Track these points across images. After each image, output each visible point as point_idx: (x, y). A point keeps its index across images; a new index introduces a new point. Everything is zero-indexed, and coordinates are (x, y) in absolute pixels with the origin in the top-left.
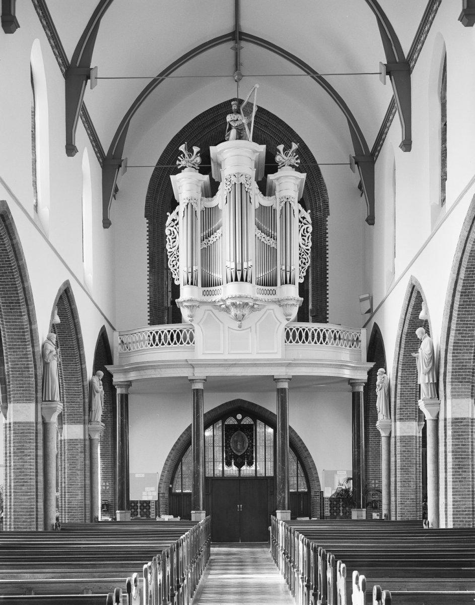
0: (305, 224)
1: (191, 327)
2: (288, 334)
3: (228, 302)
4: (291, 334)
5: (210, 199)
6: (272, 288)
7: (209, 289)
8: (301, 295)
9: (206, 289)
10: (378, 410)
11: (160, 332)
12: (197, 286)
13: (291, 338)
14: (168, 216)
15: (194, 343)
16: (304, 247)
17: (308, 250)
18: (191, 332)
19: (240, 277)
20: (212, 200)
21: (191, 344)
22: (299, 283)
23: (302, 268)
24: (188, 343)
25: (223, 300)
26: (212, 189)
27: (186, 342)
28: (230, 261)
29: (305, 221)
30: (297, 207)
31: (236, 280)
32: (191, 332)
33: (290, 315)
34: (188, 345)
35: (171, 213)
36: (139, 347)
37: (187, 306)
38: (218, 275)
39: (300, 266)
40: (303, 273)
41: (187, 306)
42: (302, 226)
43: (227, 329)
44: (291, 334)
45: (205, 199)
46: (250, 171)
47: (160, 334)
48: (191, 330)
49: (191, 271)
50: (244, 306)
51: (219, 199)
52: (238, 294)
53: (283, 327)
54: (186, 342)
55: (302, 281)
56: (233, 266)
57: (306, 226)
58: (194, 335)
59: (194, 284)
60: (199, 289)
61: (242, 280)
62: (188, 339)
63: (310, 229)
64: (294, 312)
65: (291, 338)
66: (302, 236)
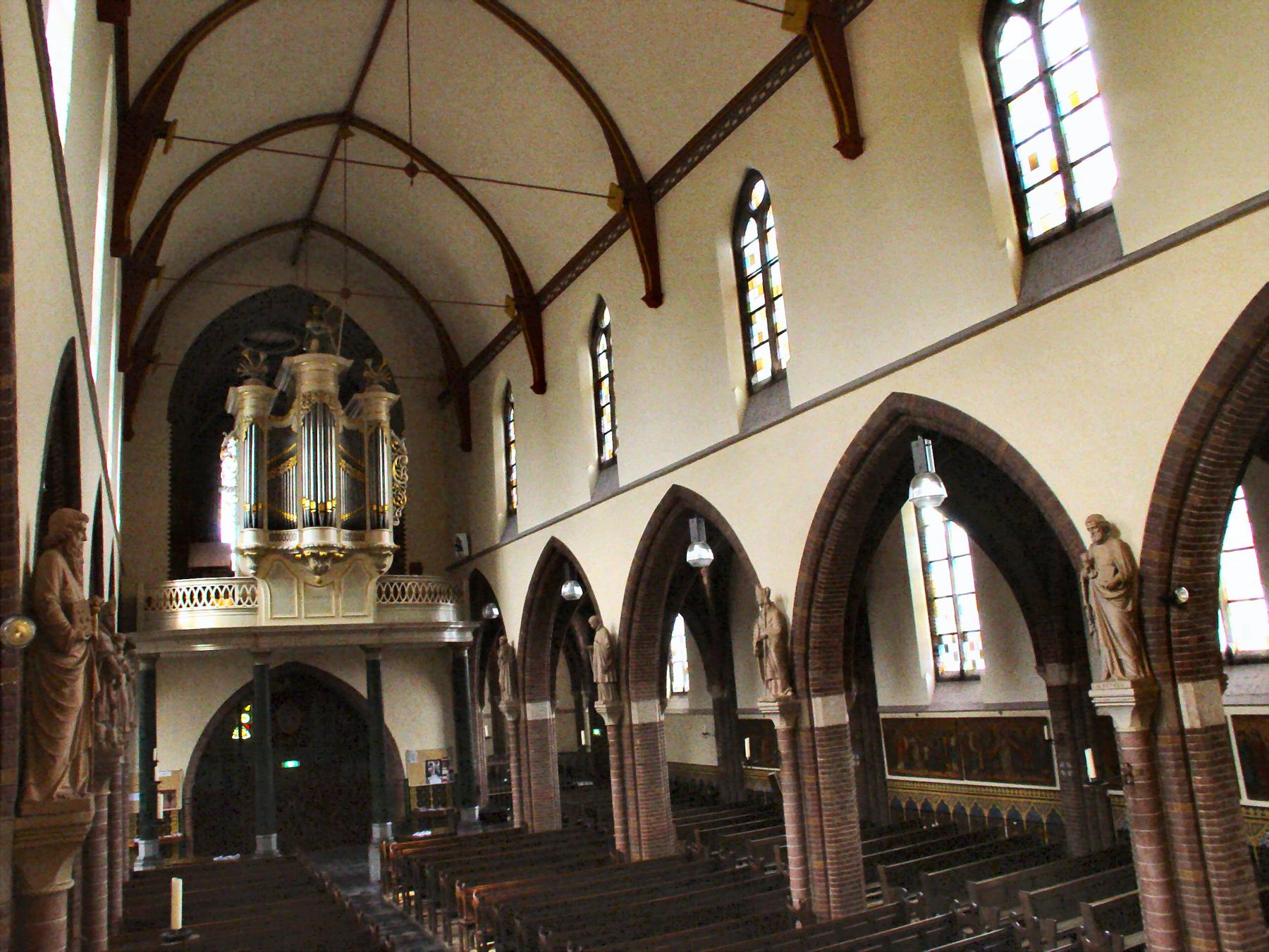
0: (400, 454)
1: (252, 581)
2: (379, 589)
3: (307, 553)
4: (384, 589)
5: (280, 418)
6: (361, 532)
7: (279, 532)
8: (395, 541)
9: (274, 532)
10: (502, 689)
13: (384, 595)
14: (224, 436)
16: (399, 482)
17: (403, 485)
19: (320, 519)
20: (282, 420)
22: (395, 528)
23: (397, 507)
24: (249, 603)
25: (298, 548)
26: (282, 406)
28: (309, 498)
29: (399, 450)
30: (387, 432)
31: (318, 524)
33: (385, 566)
35: (228, 434)
37: (250, 556)
38: (292, 517)
39: (394, 505)
40: (398, 513)
41: (250, 556)
42: (396, 457)
43: (302, 585)
44: (384, 589)
45: (273, 417)
46: (332, 387)
48: (253, 586)
50: (326, 558)
51: (294, 420)
52: (321, 543)
53: (375, 580)
55: (398, 523)
56: (314, 506)
57: (400, 457)
58: (257, 592)
60: (265, 532)
61: (325, 524)
63: (407, 460)
64: (389, 562)
65: (384, 595)
66: (396, 468)
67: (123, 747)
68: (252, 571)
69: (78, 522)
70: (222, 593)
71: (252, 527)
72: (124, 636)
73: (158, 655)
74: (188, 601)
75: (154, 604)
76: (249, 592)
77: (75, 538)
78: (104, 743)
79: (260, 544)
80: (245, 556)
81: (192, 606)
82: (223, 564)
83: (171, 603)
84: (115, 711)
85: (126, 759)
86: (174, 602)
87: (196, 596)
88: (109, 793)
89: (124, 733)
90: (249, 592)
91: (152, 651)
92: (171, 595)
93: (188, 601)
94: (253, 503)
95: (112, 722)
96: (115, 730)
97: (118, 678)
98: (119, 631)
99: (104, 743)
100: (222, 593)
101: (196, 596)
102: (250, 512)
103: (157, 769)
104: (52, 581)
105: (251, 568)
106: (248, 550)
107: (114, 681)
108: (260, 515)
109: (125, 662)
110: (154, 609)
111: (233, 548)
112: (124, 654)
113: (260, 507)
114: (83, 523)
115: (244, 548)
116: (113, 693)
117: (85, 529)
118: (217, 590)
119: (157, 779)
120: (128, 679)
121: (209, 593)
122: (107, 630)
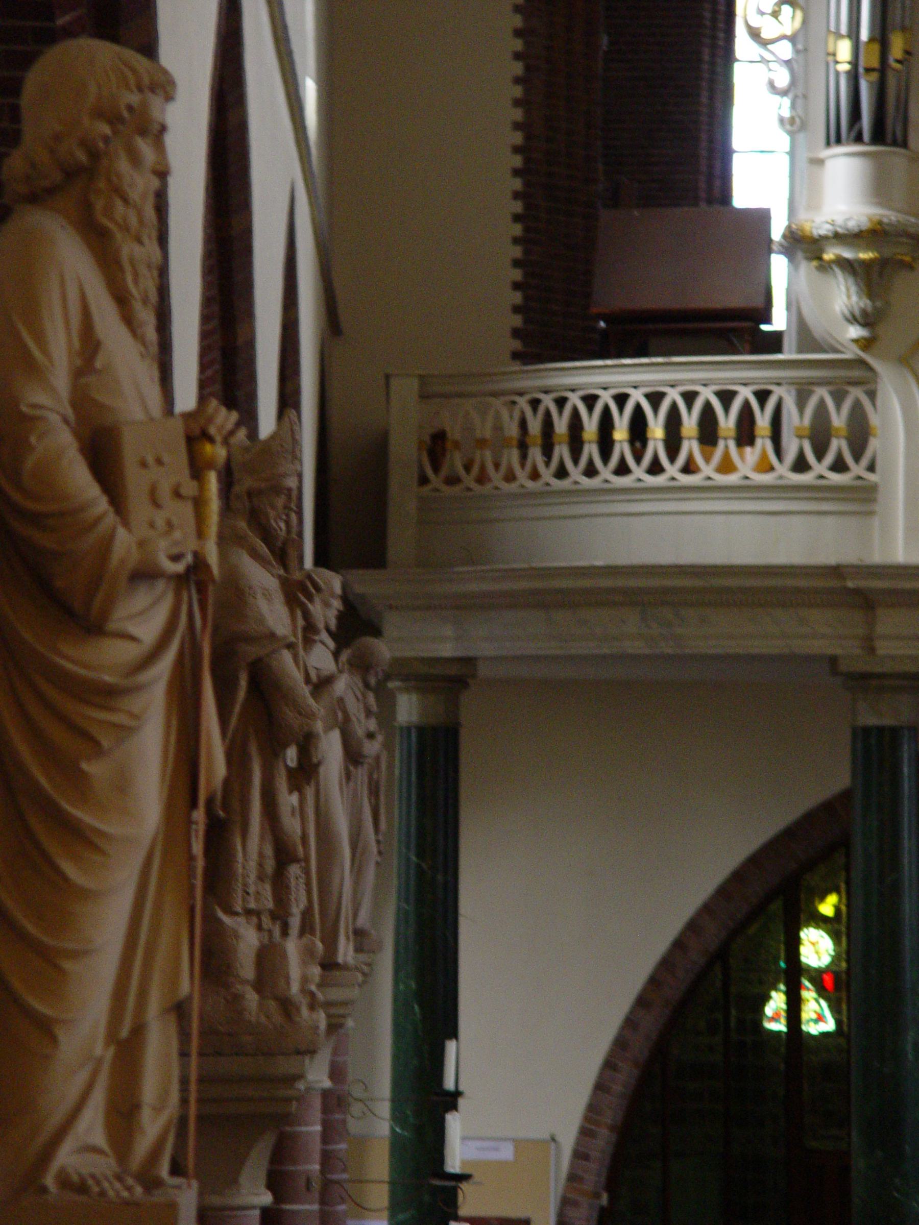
1: (855, 373)
11: (673, 395)
12: (905, 144)
15: (871, 468)
18: (857, 407)
21: (857, 469)
24: (839, 466)
27: (829, 458)
32: (857, 407)
34: (836, 478)
36: (547, 474)
37: (847, 266)
41: (847, 266)
47: (674, 408)
48: (856, 393)
49: (875, 63)
54: (829, 458)
58: (874, 420)
59: (889, 138)
62: (838, 445)
67: (321, 1019)
68: (855, 332)
69: (134, 99)
70: (727, 423)
71: (859, 139)
72: (334, 581)
73: (469, 662)
74: (591, 450)
75: (455, 461)
76: (839, 420)
77: (123, 165)
78: (252, 998)
79: (890, 216)
80: (824, 267)
81: (606, 472)
82: (735, 300)
83: (524, 457)
84: (294, 870)
85: (337, 1073)
86: (536, 454)
87: (621, 434)
88: (267, 1198)
89: (329, 965)
90: (839, 420)
91: (447, 650)
92: (523, 424)
93: (591, 450)
94: (864, 35)
95: (280, 915)
96: (292, 947)
97: (307, 743)
98: (321, 559)
99: (252, 998)
100: (727, 423)
101: (621, 434)
102: (854, 77)
103: (454, 1124)
104: (40, 338)
105: (853, 319)
106: (839, 237)
107: (291, 755)
108: (892, 82)
109: (341, 686)
110: (452, 480)
111: (777, 232)
112: (336, 655)
113: (897, 48)
114: (155, 101)
115: (824, 229)
116: (288, 800)
117: (163, 129)
118: (708, 409)
119: (454, 1163)
120: (353, 756)
121: (673, 422)
122: (263, 549)
